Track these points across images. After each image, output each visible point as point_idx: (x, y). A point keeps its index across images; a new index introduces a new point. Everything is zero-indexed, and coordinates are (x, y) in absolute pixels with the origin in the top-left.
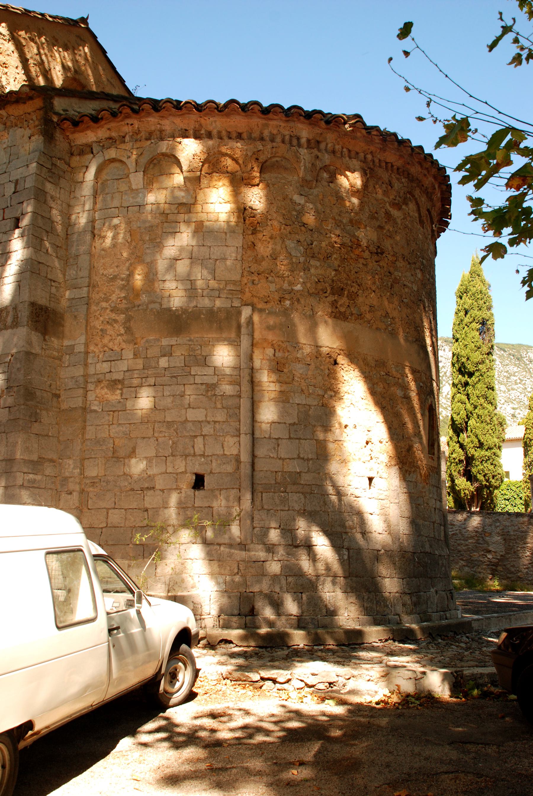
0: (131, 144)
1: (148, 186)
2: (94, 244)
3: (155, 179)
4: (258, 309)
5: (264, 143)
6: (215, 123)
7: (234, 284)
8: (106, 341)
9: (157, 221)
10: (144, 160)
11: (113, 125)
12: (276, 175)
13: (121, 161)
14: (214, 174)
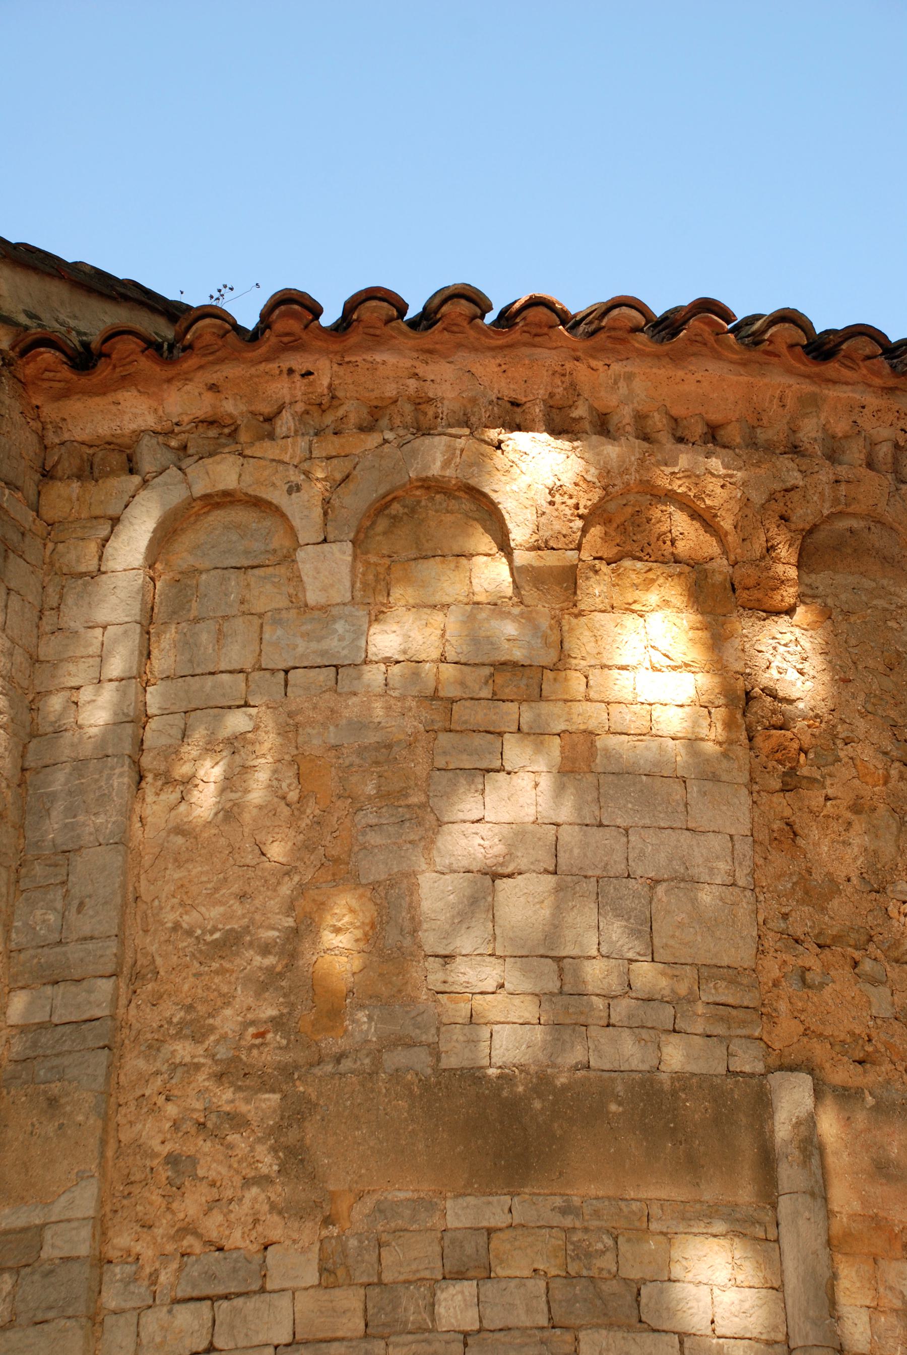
0: (302, 443)
1: (373, 596)
2: (137, 807)
3: (397, 572)
4: (834, 1089)
5: (805, 463)
6: (632, 383)
7: (732, 982)
8: (190, 1205)
9: (411, 725)
10: (355, 502)
11: (231, 371)
12: (852, 580)
13: (257, 503)
14: (627, 563)
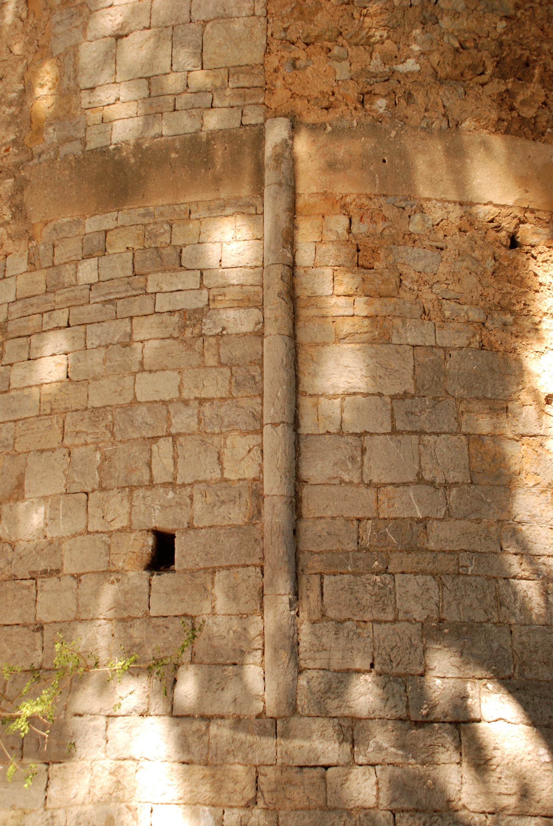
4: (307, 125)
